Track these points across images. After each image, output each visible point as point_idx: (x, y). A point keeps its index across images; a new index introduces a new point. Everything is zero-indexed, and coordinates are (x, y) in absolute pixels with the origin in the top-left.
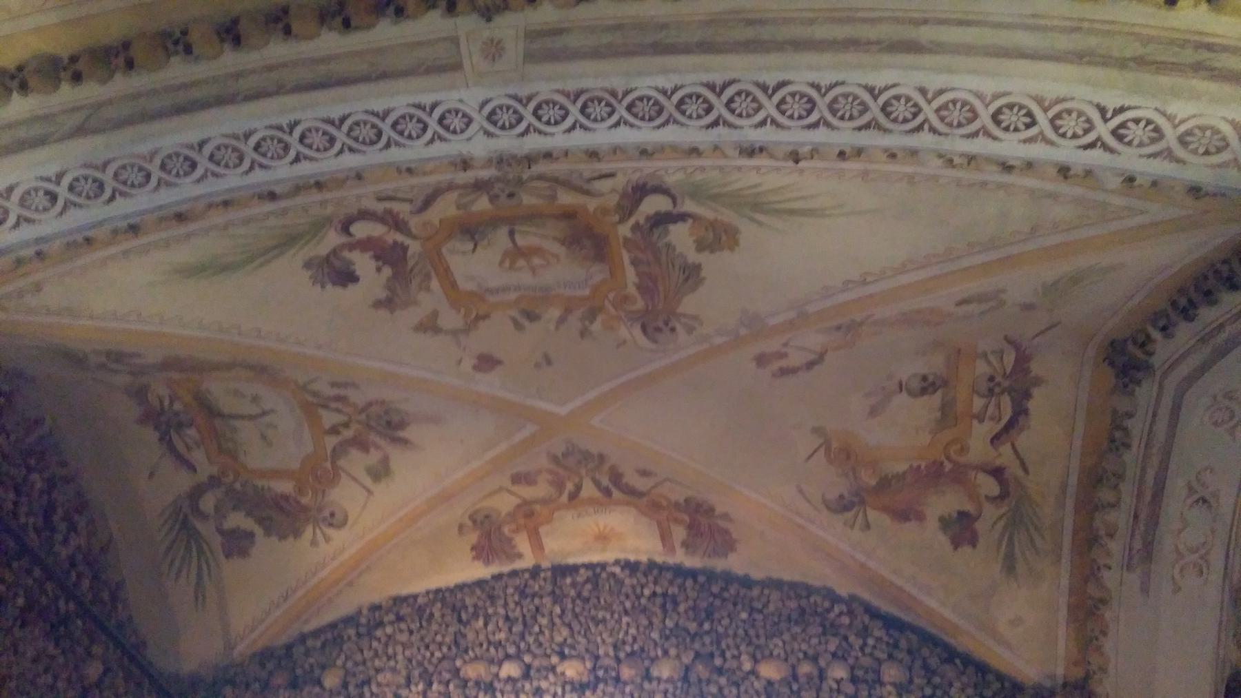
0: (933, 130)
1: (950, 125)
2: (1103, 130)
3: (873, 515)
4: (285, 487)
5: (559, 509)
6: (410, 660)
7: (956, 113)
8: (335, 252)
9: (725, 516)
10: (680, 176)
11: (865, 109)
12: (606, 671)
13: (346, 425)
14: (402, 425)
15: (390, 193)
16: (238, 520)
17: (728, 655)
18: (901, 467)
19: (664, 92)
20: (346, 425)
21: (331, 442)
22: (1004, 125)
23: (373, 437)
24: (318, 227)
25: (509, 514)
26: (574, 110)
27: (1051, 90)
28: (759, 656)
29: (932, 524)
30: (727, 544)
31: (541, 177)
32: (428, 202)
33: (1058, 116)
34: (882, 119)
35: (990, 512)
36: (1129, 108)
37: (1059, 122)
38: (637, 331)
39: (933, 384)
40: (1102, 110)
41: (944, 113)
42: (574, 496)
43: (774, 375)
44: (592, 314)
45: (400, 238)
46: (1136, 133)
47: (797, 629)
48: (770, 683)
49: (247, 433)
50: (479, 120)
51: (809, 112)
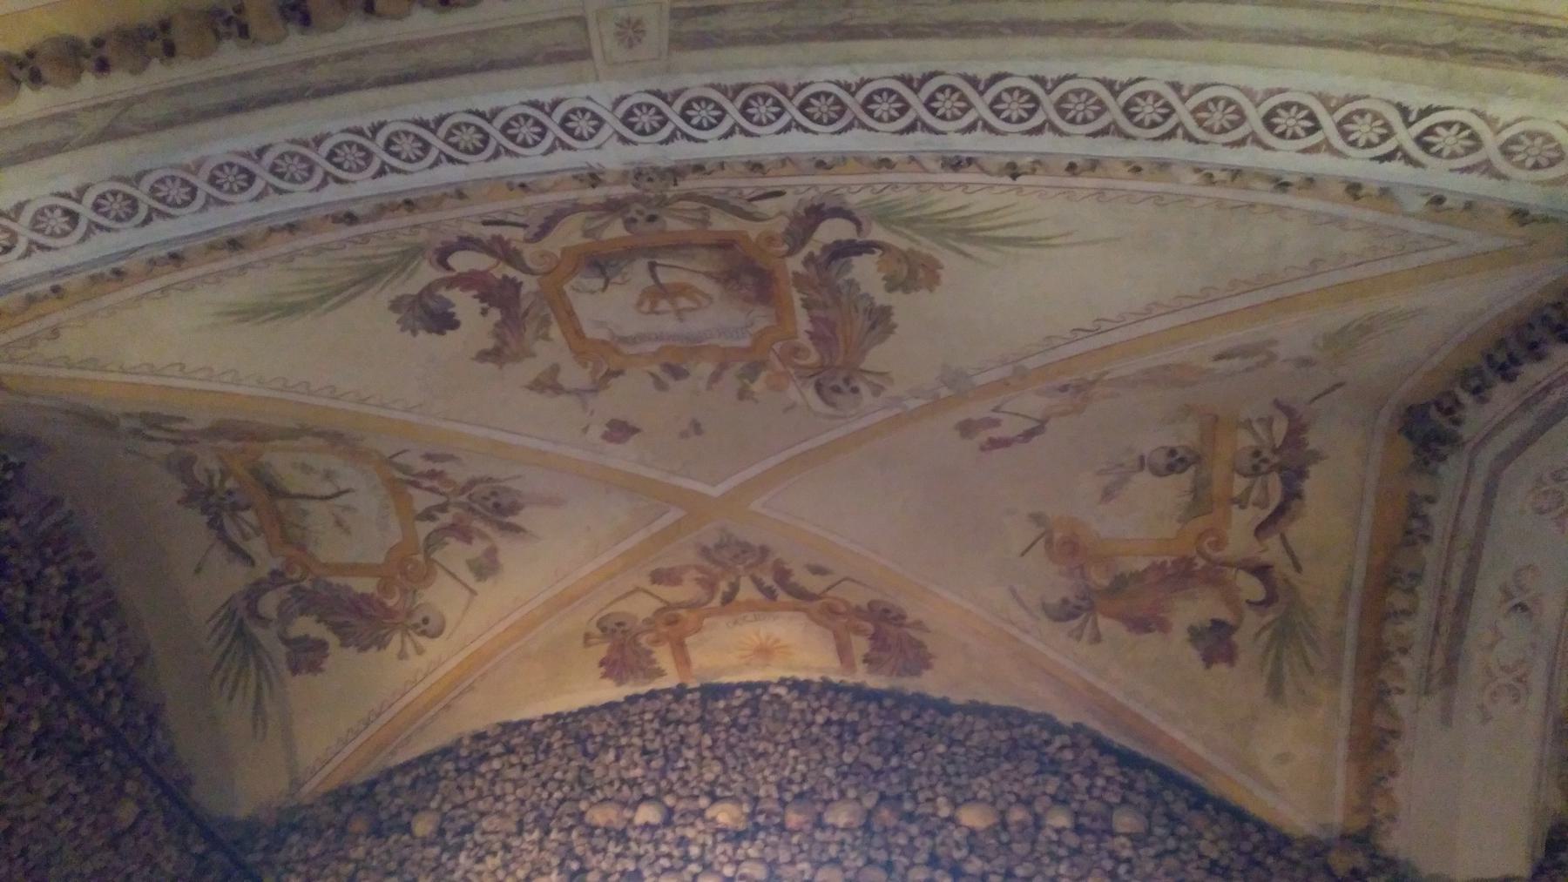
0: (1189, 137)
1: (1210, 130)
2: (1404, 137)
3: (1104, 623)
4: (364, 585)
5: (708, 616)
6: (522, 802)
7: (1218, 115)
8: (429, 289)
9: (919, 625)
10: (865, 195)
11: (1102, 108)
13: (443, 508)
14: (514, 509)
15: (499, 217)
16: (306, 626)
17: (921, 796)
18: (1141, 564)
19: (846, 87)
20: (443, 508)
21: (424, 529)
22: (1278, 130)
23: (478, 524)
24: (411, 254)
25: (647, 621)
26: (733, 109)
27: (1340, 85)
29: (1179, 634)
30: (917, 658)
31: (689, 196)
32: (545, 229)
33: (1348, 119)
34: (1123, 122)
35: (1252, 621)
36: (1438, 109)
37: (1349, 127)
38: (810, 393)
39: (1182, 460)
40: (1404, 111)
41: (1203, 115)
42: (728, 599)
43: (983, 449)
44: (753, 370)
45: (511, 272)
46: (1447, 140)
47: (1006, 766)
48: (973, 832)
49: (319, 515)
50: (613, 123)
51: (1032, 112)
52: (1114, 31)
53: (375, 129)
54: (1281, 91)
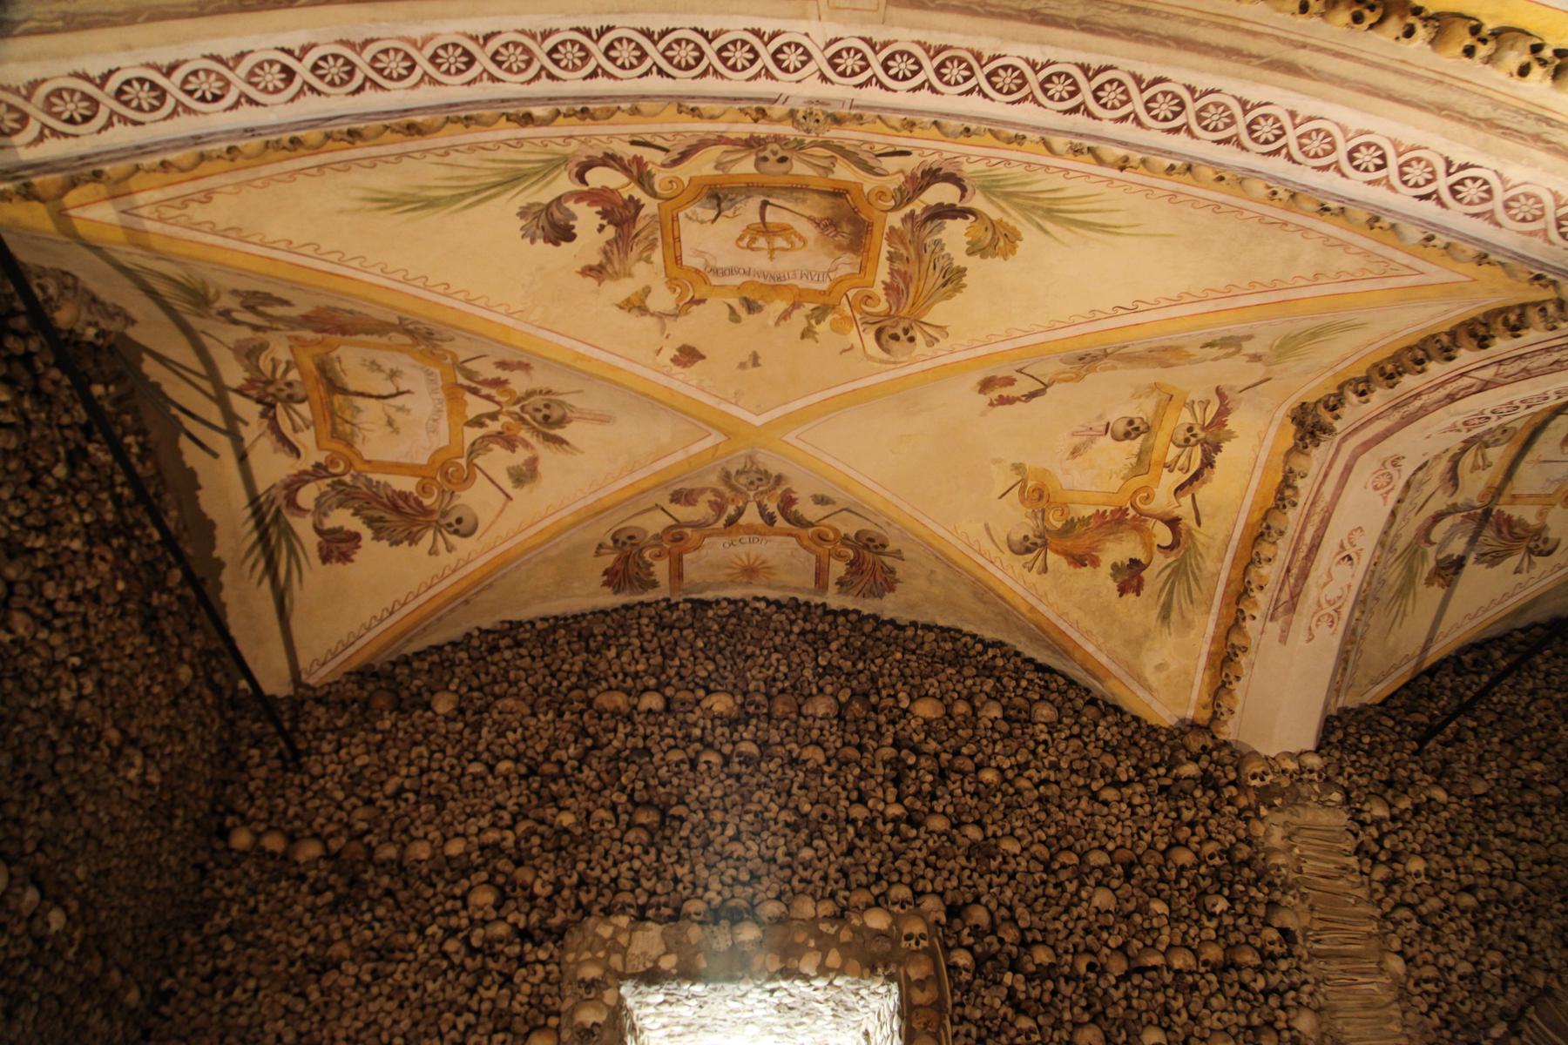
0: (1289, 157)
1: (1306, 154)
2: (1442, 184)
3: (1051, 557)
4: (407, 484)
5: (710, 535)
6: (535, 689)
7: (1316, 143)
8: (559, 200)
9: (898, 554)
10: (982, 166)
11: (1232, 121)
12: (757, 707)
13: (494, 416)
14: (562, 422)
15: (648, 138)
17: (884, 693)
18: (1088, 511)
19: (1033, 65)
20: (494, 416)
21: (472, 434)
23: (524, 434)
24: (553, 165)
25: (657, 537)
26: (929, 67)
27: (1409, 135)
28: (915, 695)
29: (1105, 569)
30: (886, 582)
31: (825, 144)
32: (684, 156)
33: (1407, 163)
35: (1160, 561)
36: (1473, 166)
38: (870, 338)
39: (1137, 429)
42: (731, 522)
43: (991, 404)
44: (820, 313)
45: (638, 193)
46: (1471, 191)
47: (950, 671)
48: (927, 722)
49: (371, 413)
50: (820, 61)
51: (1176, 115)
52: (1257, 62)
53: (602, 32)
54: (1368, 133)
